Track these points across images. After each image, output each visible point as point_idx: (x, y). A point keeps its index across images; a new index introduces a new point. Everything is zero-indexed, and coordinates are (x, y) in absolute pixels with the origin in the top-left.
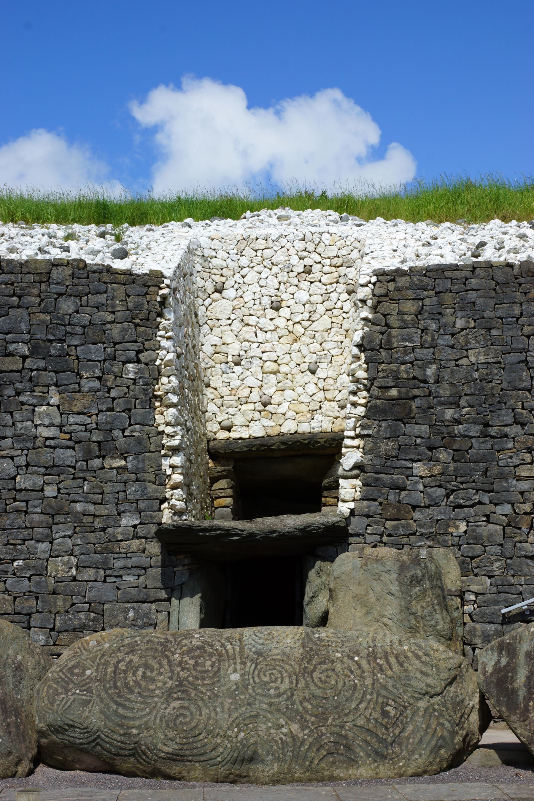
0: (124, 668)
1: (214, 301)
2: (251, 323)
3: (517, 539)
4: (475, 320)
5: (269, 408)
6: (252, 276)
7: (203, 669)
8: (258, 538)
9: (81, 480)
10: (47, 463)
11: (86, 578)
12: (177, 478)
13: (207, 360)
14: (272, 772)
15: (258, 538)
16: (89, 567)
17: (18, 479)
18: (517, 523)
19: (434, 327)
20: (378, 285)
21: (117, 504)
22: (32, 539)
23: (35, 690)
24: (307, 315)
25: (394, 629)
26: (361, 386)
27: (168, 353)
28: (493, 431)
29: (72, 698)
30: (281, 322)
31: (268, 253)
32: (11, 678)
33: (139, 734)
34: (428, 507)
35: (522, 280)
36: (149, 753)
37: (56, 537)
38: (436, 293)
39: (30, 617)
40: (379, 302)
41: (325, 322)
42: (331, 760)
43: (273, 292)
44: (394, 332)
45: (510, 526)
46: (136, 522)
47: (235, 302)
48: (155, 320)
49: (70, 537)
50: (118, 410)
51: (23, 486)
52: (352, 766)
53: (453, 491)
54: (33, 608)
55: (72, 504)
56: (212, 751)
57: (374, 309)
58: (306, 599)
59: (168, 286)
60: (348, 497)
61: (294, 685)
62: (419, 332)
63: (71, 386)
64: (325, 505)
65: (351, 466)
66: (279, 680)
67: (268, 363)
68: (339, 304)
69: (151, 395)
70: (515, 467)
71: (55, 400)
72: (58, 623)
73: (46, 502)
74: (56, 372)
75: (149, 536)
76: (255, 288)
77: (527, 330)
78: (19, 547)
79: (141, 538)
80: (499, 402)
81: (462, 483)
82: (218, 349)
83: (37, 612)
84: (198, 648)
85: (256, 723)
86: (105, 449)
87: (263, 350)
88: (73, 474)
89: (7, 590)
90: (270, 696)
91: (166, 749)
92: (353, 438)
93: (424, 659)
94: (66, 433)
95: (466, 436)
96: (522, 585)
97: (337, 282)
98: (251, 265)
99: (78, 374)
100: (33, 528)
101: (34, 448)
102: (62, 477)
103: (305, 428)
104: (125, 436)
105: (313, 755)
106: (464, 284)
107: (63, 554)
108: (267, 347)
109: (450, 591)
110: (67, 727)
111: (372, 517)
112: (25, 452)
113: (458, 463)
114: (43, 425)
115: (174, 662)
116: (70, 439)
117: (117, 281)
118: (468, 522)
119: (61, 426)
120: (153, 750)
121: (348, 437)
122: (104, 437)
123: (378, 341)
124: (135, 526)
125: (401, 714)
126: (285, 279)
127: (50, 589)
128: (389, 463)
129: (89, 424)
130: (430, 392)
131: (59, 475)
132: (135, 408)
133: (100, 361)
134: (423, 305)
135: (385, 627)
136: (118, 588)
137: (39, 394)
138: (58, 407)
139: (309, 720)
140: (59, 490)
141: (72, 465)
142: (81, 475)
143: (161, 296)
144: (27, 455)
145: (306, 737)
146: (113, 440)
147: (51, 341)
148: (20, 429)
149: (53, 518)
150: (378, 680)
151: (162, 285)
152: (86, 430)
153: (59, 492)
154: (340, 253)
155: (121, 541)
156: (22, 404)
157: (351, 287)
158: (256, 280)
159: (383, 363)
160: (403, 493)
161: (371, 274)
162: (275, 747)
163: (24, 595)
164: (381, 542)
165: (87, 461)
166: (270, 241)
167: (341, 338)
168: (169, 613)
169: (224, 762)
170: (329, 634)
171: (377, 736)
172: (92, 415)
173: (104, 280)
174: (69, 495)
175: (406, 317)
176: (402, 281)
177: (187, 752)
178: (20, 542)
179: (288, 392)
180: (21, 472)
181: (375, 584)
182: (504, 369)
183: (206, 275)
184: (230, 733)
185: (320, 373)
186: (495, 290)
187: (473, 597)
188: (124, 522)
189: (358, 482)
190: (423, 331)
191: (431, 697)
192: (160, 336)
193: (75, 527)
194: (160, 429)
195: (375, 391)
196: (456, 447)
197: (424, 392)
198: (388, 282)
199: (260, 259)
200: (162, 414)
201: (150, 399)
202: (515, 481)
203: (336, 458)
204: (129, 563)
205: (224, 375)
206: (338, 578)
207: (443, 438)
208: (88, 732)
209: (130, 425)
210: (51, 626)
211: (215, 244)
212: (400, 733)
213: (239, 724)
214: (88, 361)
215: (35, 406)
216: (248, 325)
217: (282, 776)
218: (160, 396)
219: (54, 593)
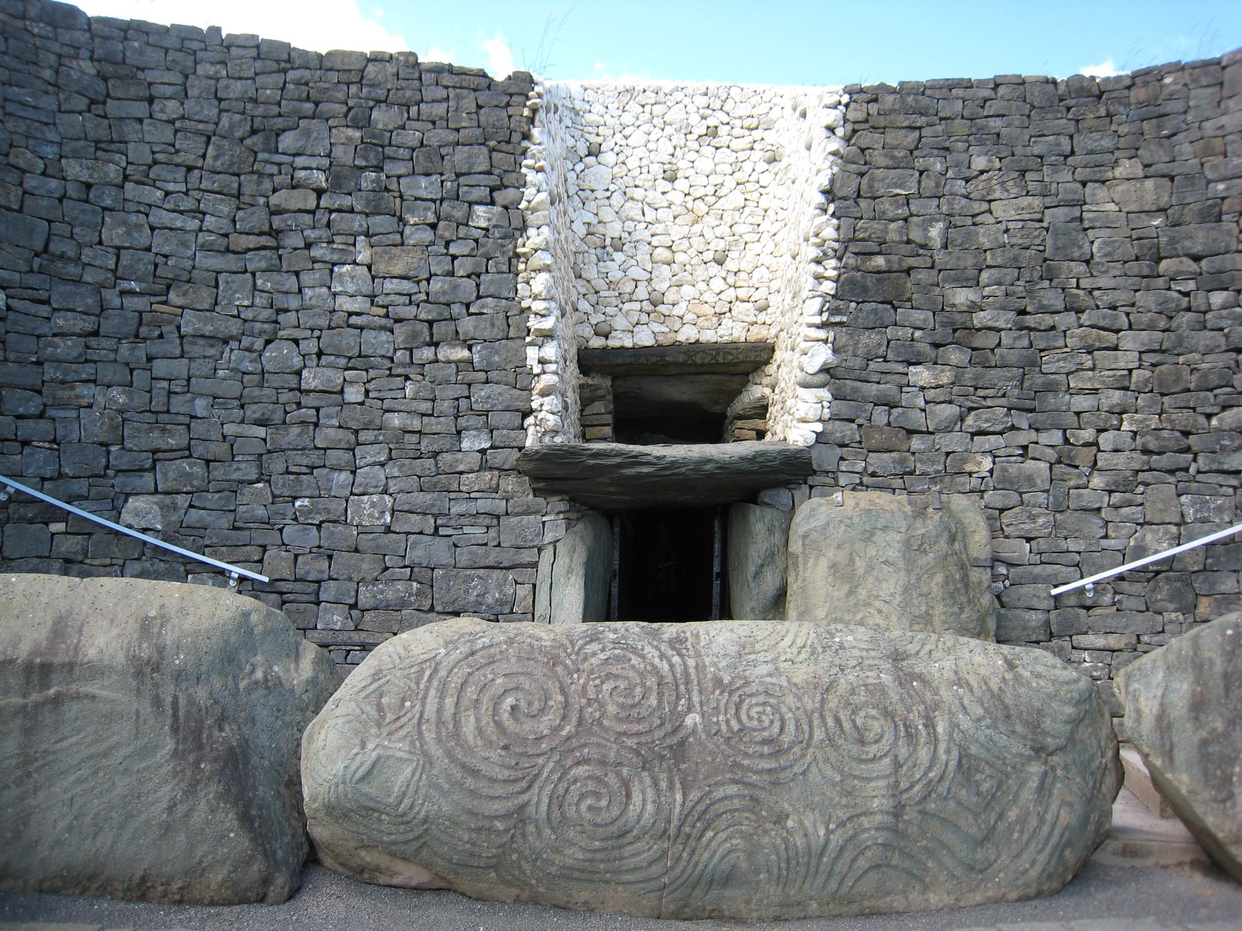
0: (475, 697)
1: (587, 167)
2: (636, 196)
3: (1072, 483)
4: (1000, 159)
5: (661, 308)
6: (637, 138)
7: (630, 701)
10: (349, 349)
11: (406, 528)
12: (548, 380)
13: (578, 242)
15: (683, 470)
17: (305, 373)
18: (1071, 458)
19: (938, 167)
20: (852, 105)
21: (457, 418)
22: (324, 466)
23: (306, 734)
24: (710, 190)
25: (894, 619)
26: (830, 253)
27: (538, 191)
28: (1030, 320)
29: (374, 754)
30: (676, 197)
31: (658, 109)
33: (507, 830)
34: (932, 433)
35: (1071, 102)
36: (526, 866)
37: (362, 464)
38: (941, 119)
39: (320, 587)
40: (855, 131)
41: (736, 199)
43: (667, 159)
44: (879, 173)
45: (1059, 462)
46: (487, 445)
47: (616, 169)
48: (519, 143)
49: (382, 465)
53: (971, 409)
54: (323, 572)
56: (650, 865)
57: (847, 140)
58: (752, 569)
59: (540, 96)
60: (811, 416)
61: (807, 736)
62: (917, 174)
64: (738, 440)
65: (817, 369)
66: (777, 724)
67: (658, 250)
68: (754, 177)
69: (511, 254)
70: (1068, 374)
71: (363, 256)
72: (361, 597)
73: (347, 410)
74: (367, 215)
75: (506, 467)
76: (641, 152)
77: (1081, 174)
79: (491, 469)
80: (1041, 278)
81: (985, 398)
82: (592, 230)
83: (330, 579)
84: (618, 659)
87: (651, 232)
88: (390, 369)
90: (762, 756)
91: (558, 859)
92: (818, 327)
93: (1034, 685)
95: (990, 329)
96: (1079, 553)
97: (752, 149)
98: (637, 123)
99: (401, 219)
100: (325, 449)
101: (330, 328)
102: (372, 373)
103: (708, 336)
104: (470, 315)
105: (845, 869)
106: (983, 107)
107: (371, 490)
108: (659, 228)
109: (976, 559)
110: (364, 813)
111: (846, 446)
112: (317, 333)
113: (979, 369)
114: (345, 293)
115: (573, 687)
116: (387, 316)
117: (464, 84)
118: (995, 457)
120: (536, 860)
121: (810, 326)
122: (439, 314)
123: (854, 187)
124: (483, 452)
125: (998, 788)
126: (682, 144)
127: (350, 544)
128: (872, 366)
130: (933, 263)
131: (367, 371)
133: (434, 201)
134: (920, 138)
135: (877, 616)
136: (456, 546)
140: (367, 392)
141: (390, 355)
142: (400, 371)
143: (529, 107)
144: (319, 338)
146: (451, 319)
147: (363, 169)
149: (357, 437)
150: (958, 726)
151: (531, 94)
152: (411, 303)
154: (755, 112)
157: (768, 155)
158: (643, 142)
159: (861, 218)
160: (895, 412)
161: (841, 92)
162: (773, 857)
164: (861, 484)
165: (411, 350)
166: (661, 94)
167: (759, 220)
168: (534, 586)
169: (674, 886)
170: (860, 637)
173: (444, 83)
175: (896, 153)
176: (889, 100)
177: (602, 866)
178: (305, 470)
179: (686, 289)
180: (308, 363)
181: (859, 546)
182: (1047, 230)
183: (578, 134)
184: (687, 829)
185: (731, 265)
186: (1029, 116)
187: (1002, 570)
188: (465, 445)
189: (825, 394)
190: (921, 175)
191: (1051, 754)
192: (527, 167)
193: (391, 450)
194: (524, 304)
195: (850, 260)
196: (976, 344)
197: (925, 262)
198: (868, 102)
199: (647, 116)
201: (510, 259)
202: (1067, 397)
203: (751, 378)
204: (472, 507)
205: (601, 264)
206: (805, 537)
207: (955, 331)
208: (408, 823)
209: (479, 297)
210: (352, 601)
211: (590, 95)
212: (996, 822)
214: (417, 199)
215: (334, 264)
216: (632, 199)
218: (524, 254)
219: (356, 550)
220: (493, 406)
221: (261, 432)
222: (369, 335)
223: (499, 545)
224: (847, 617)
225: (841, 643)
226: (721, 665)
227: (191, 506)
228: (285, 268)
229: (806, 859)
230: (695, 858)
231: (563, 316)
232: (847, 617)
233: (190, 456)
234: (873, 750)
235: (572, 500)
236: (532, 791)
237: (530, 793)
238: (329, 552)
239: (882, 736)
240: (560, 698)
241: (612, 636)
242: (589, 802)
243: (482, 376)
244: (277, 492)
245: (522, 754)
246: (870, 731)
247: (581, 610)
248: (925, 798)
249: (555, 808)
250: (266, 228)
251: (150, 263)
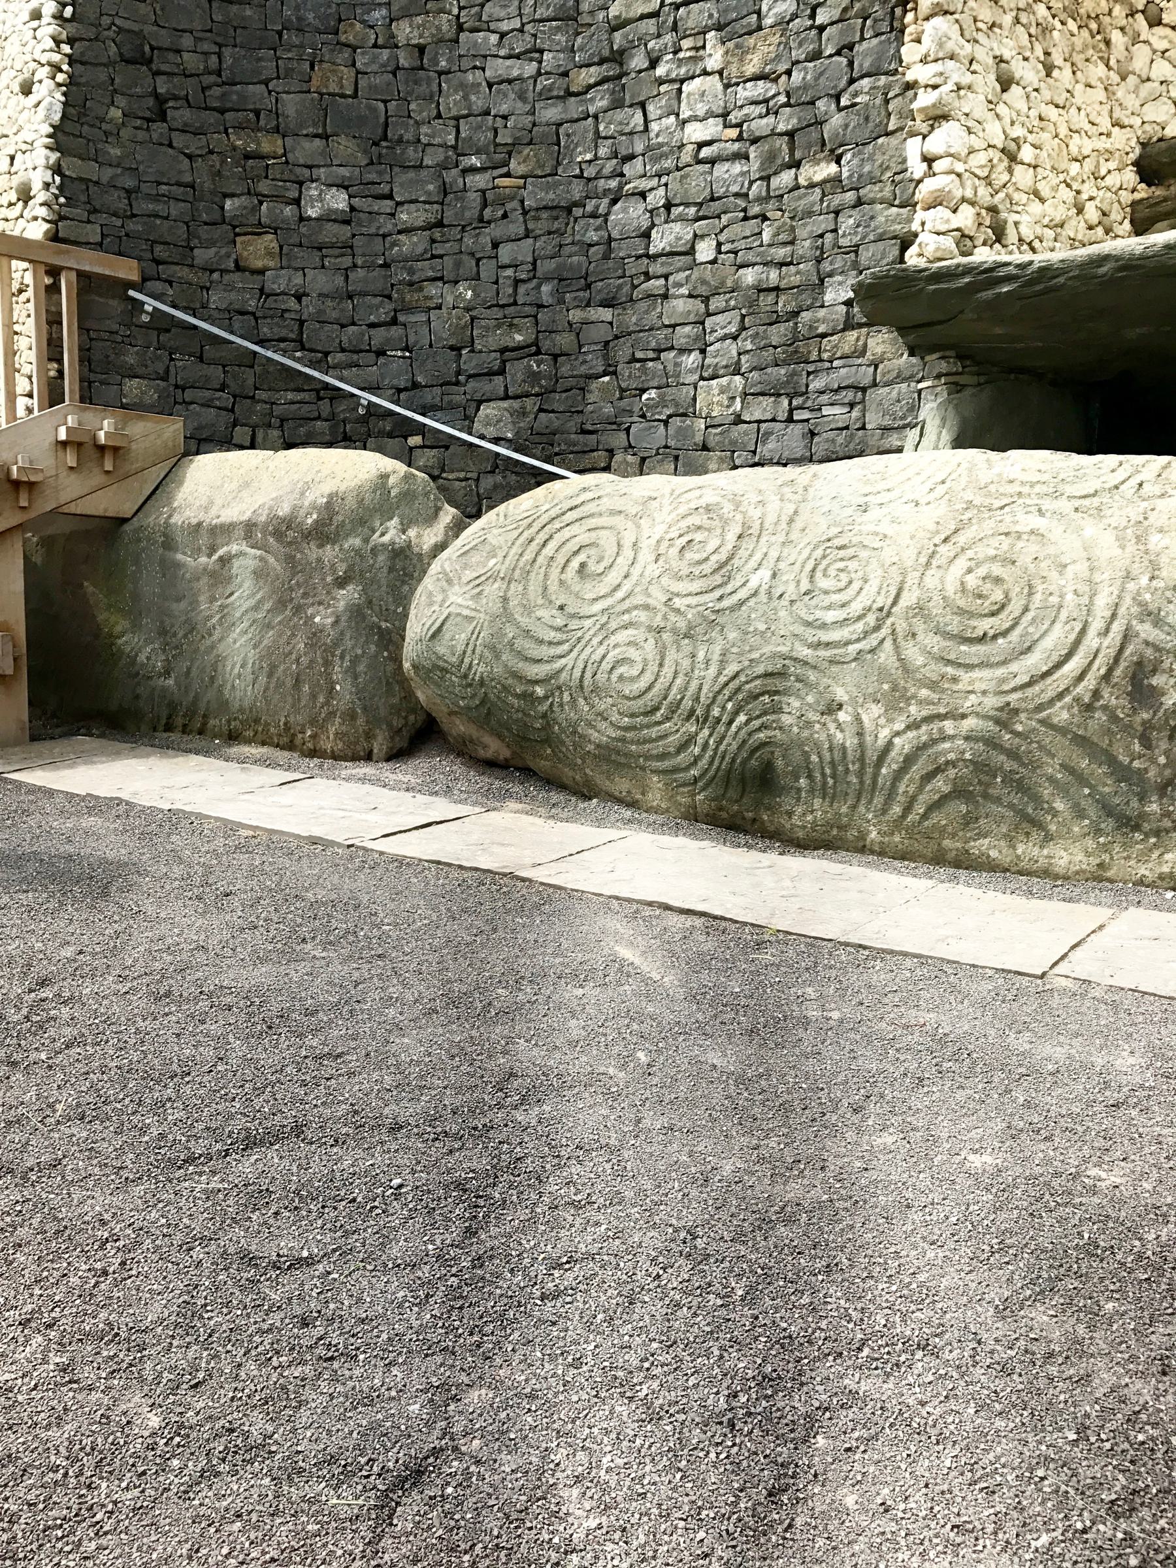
8: (1061, 280)
9: (759, 220)
11: (757, 415)
14: (809, 818)
15: (1061, 280)
16: (763, 394)
22: (672, 348)
32: (385, 570)
33: (546, 697)
42: (963, 808)
49: (735, 338)
50: (828, 53)
51: (662, 246)
52: (1027, 834)
55: (741, 271)
61: (890, 601)
63: (744, 22)
71: (715, 58)
73: (696, 274)
78: (650, 364)
85: (777, 693)
86: (798, 144)
88: (745, 210)
89: (630, 446)
90: (824, 626)
94: (731, 127)
100: (674, 326)
101: (678, 169)
104: (840, 109)
107: (721, 372)
112: (664, 180)
116: (740, 138)
119: (725, 115)
122: (799, 119)
129: (774, 96)
131: (719, 217)
132: (862, 39)
137: (688, 54)
138: (720, 73)
139: (914, 697)
140: (719, 244)
141: (744, 190)
142: (755, 209)
144: (666, 185)
145: (897, 740)
148: (657, 136)
149: (707, 306)
153: (720, 252)
155: (823, 336)
156: (661, 82)
163: (658, 454)
165: (767, 179)
171: (1112, 761)
172: (779, 76)
174: (736, 253)
178: (651, 355)
188: (829, 297)
193: (743, 317)
194: (910, 76)
200: (919, 41)
208: (470, 685)
209: (852, 81)
213: (738, 690)
215: (682, 81)
217: (835, 832)
219: (705, 448)
220: (864, 238)
221: (606, 314)
222: (720, 169)
223: (863, 428)
227: (541, 410)
228: (627, 103)
229: (857, 766)
230: (722, 748)
231: (1006, 83)
233: (538, 353)
235: (960, 357)
238: (675, 452)
239: (1003, 607)
243: (850, 196)
244: (624, 385)
248: (1051, 702)
249: (588, 675)
250: (606, 53)
251: (488, 129)
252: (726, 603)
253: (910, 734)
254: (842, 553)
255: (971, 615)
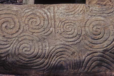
7: (36, 24)
66: (73, 30)
213: (54, 51)
224: (101, 3)
225: (92, 9)
226: (60, 15)
230: (52, 63)
232: (101, 3)
234: (98, 36)
236: (11, 47)
237: (10, 48)
239: (100, 33)
240: (19, 24)
241: (33, 8)
242: (25, 49)
245: (8, 38)
246: (97, 32)
247: (34, 2)
249: (17, 51)
252: (46, 34)
253: (89, 56)
254: (68, 24)
255: (95, 35)
